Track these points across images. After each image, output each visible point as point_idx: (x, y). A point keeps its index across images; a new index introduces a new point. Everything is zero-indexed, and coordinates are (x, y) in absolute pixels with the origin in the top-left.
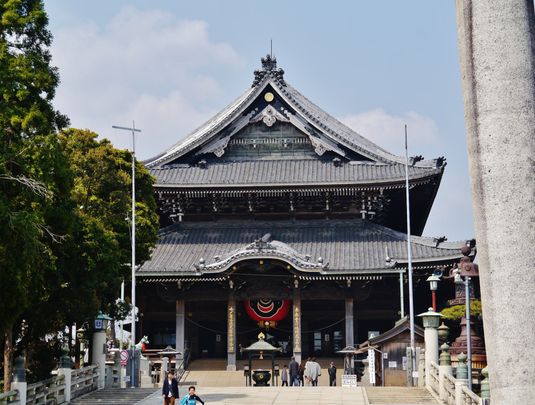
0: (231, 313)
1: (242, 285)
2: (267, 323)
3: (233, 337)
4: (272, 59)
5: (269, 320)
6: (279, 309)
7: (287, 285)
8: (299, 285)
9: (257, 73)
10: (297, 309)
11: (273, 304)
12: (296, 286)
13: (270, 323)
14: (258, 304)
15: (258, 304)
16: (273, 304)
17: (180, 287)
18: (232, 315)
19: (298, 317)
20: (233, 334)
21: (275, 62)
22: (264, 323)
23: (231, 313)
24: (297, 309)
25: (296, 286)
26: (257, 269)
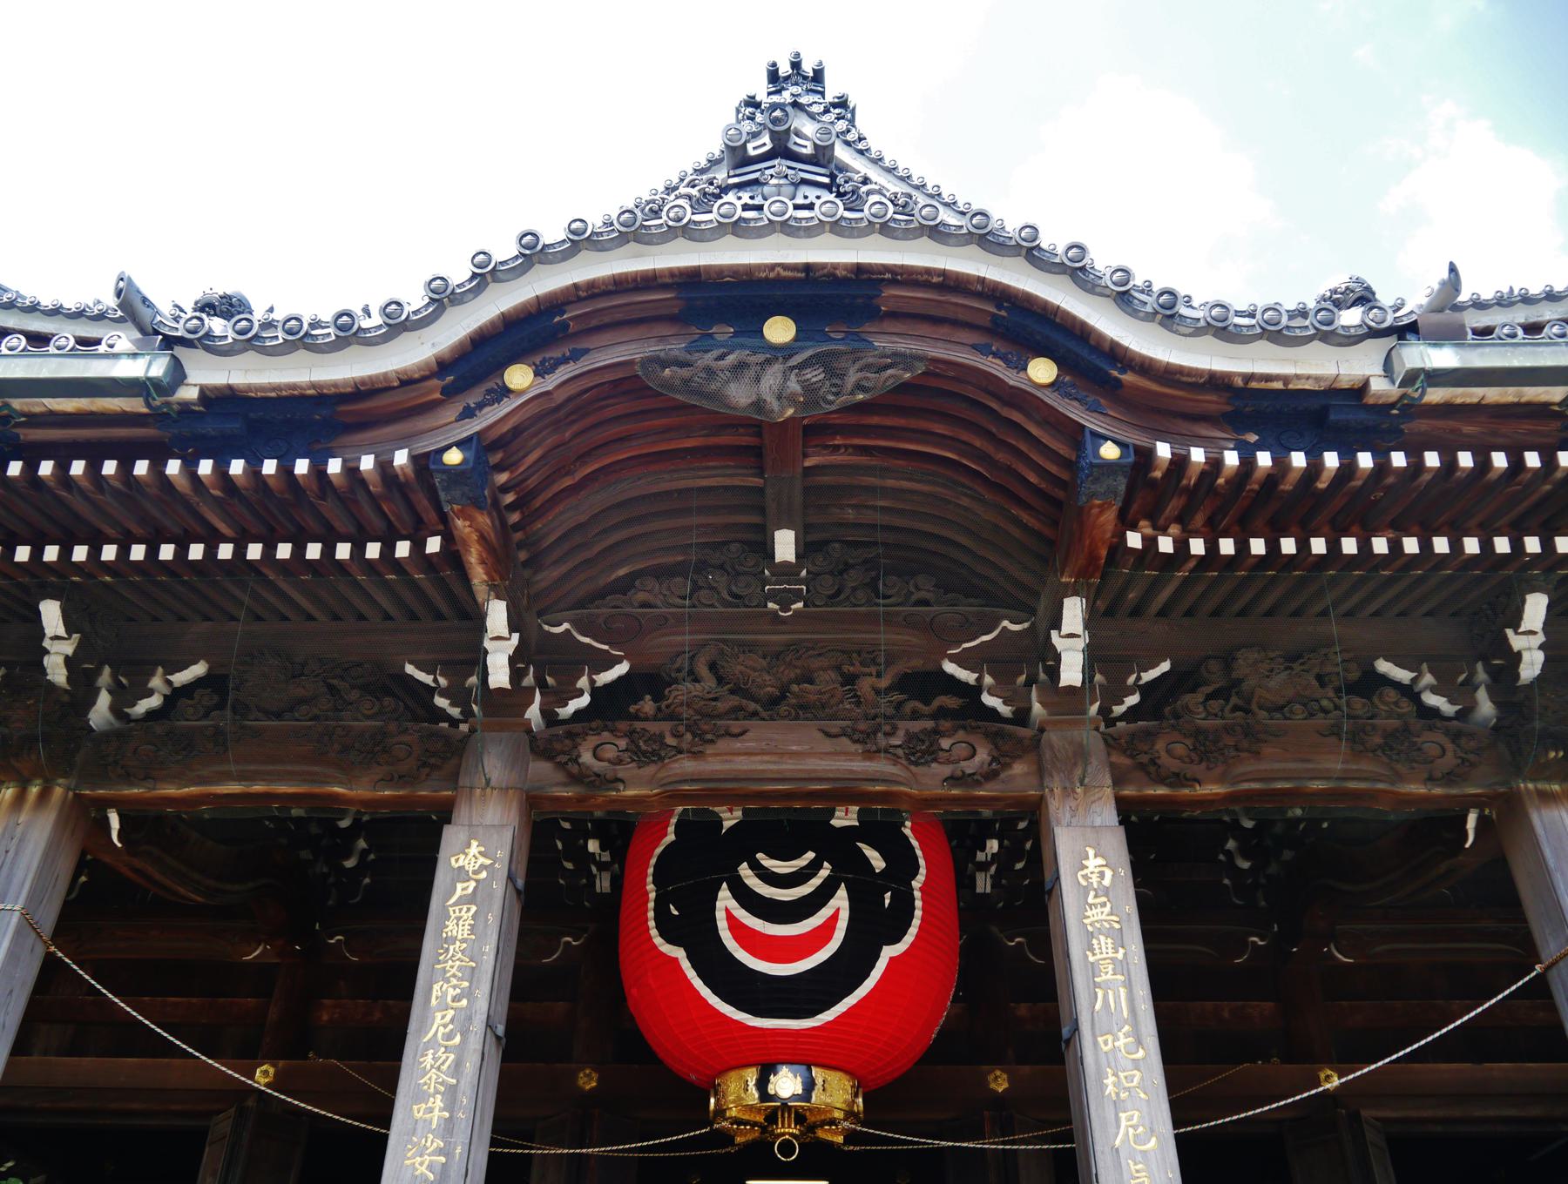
0: (463, 889)
1: (595, 692)
2: (786, 1084)
3: (448, 1126)
4: (808, 68)
5: (802, 1053)
6: (889, 952)
7: (977, 689)
8: (1094, 658)
9: (751, 102)
10: (1093, 863)
11: (840, 901)
12: (1071, 673)
13: (809, 1086)
14: (725, 900)
15: (725, 900)
16: (840, 901)
17: (56, 671)
18: (468, 913)
19: (1120, 942)
20: (451, 1094)
21: (818, 76)
22: (762, 1084)
23: (463, 889)
24: (1093, 863)
25: (1071, 673)
26: (740, 394)
